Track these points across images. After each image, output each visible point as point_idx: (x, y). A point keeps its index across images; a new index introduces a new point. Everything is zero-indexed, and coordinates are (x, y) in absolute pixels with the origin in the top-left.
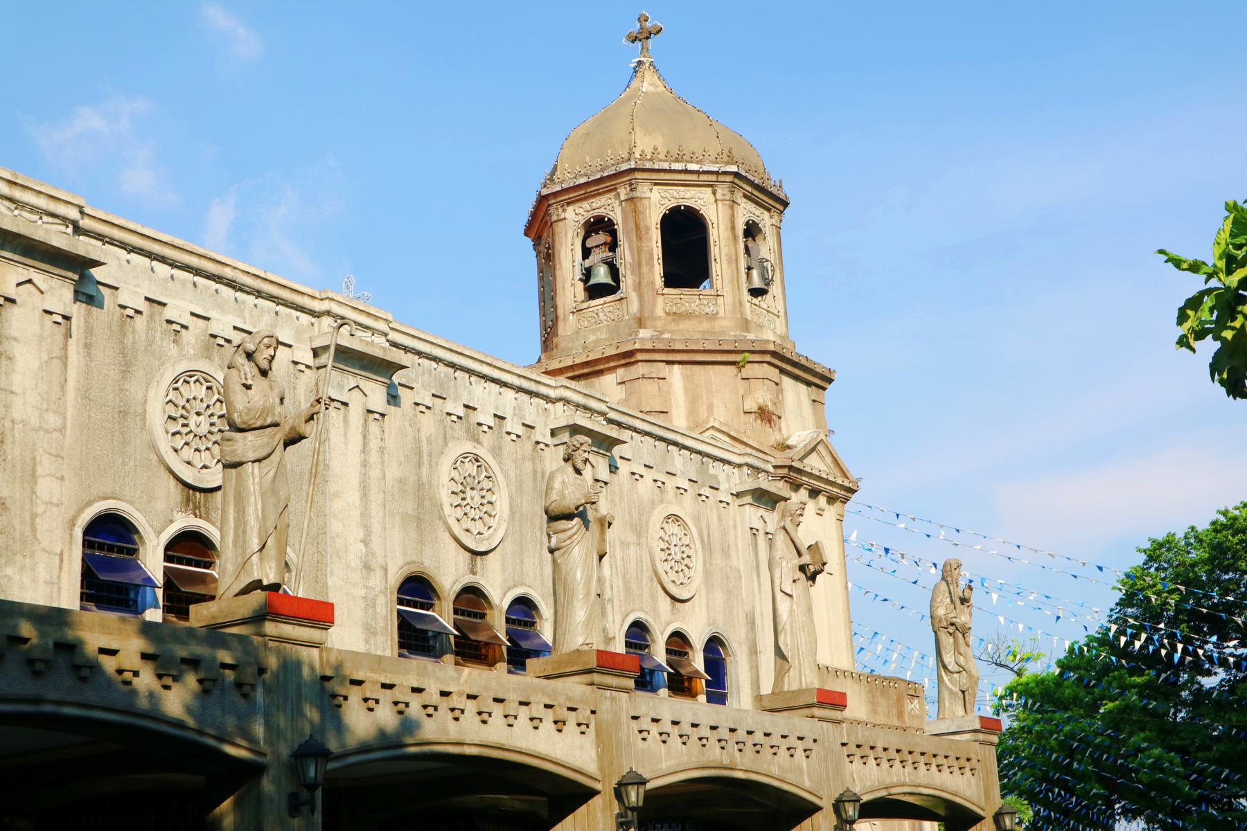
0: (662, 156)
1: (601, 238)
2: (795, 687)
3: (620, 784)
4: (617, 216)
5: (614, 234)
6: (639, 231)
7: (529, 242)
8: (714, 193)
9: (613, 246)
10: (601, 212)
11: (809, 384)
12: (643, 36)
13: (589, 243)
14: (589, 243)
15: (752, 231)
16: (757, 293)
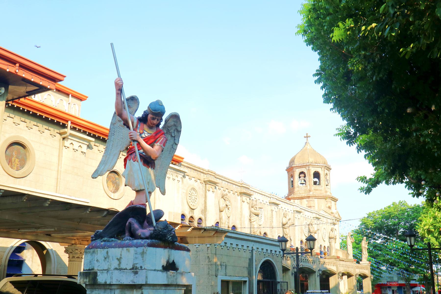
0: (314, 163)
1: (303, 175)
2: (350, 258)
3: (339, 273)
4: (306, 172)
5: (305, 175)
6: (310, 175)
7: (286, 172)
8: (322, 169)
9: (305, 177)
10: (303, 171)
11: (334, 201)
12: (307, 137)
13: (301, 176)
14: (301, 176)
15: (327, 174)
16: (327, 185)
